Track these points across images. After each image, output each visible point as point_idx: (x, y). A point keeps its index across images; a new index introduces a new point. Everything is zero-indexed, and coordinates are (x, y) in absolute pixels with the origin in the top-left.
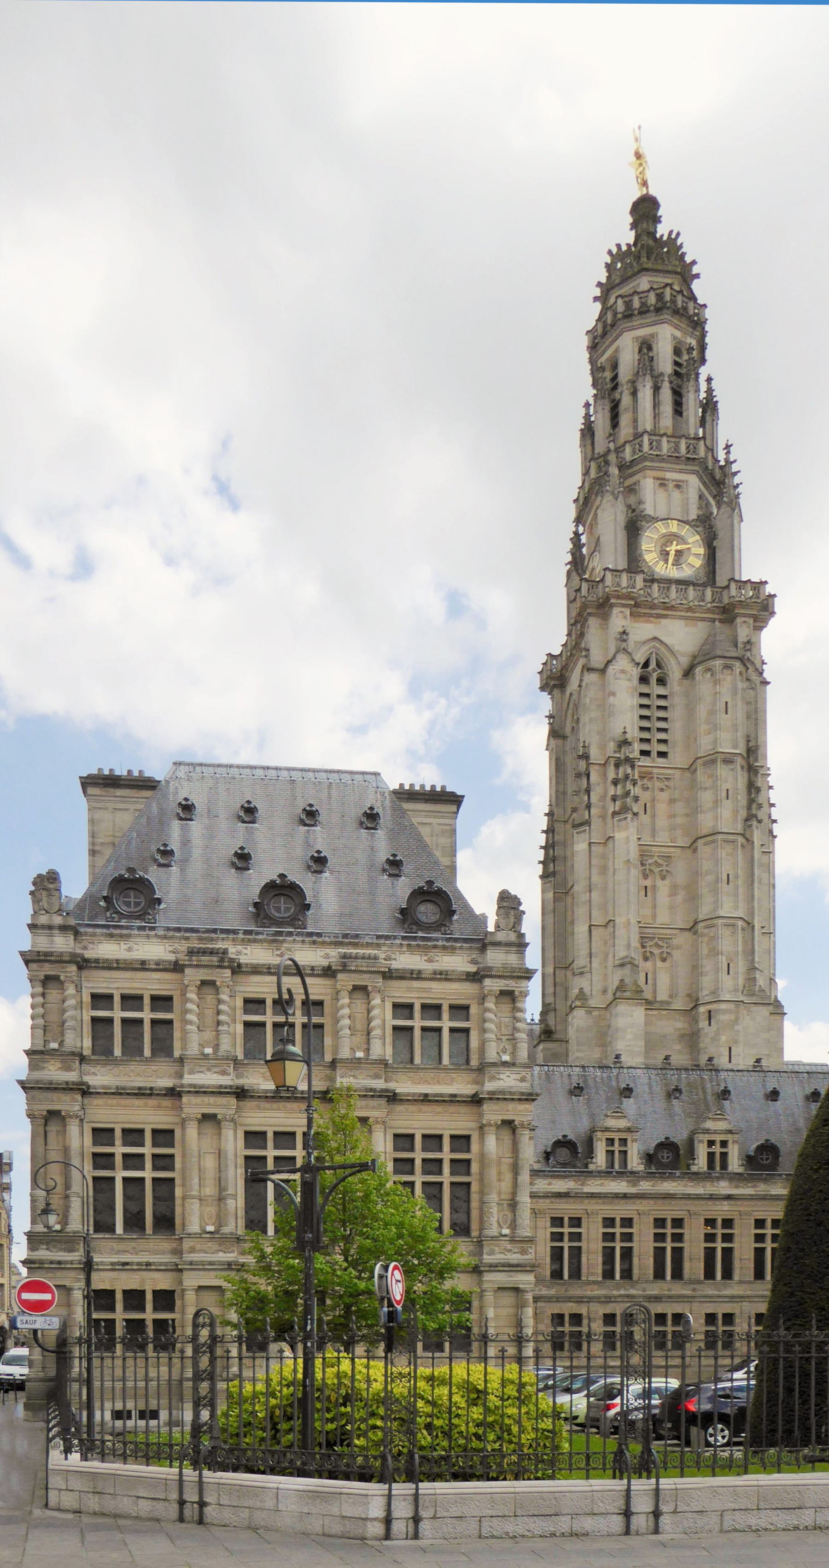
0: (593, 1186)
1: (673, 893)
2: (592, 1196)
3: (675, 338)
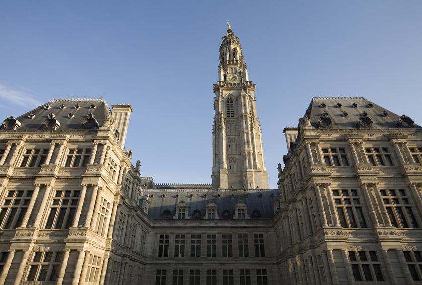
0: (204, 225)
2: (202, 227)
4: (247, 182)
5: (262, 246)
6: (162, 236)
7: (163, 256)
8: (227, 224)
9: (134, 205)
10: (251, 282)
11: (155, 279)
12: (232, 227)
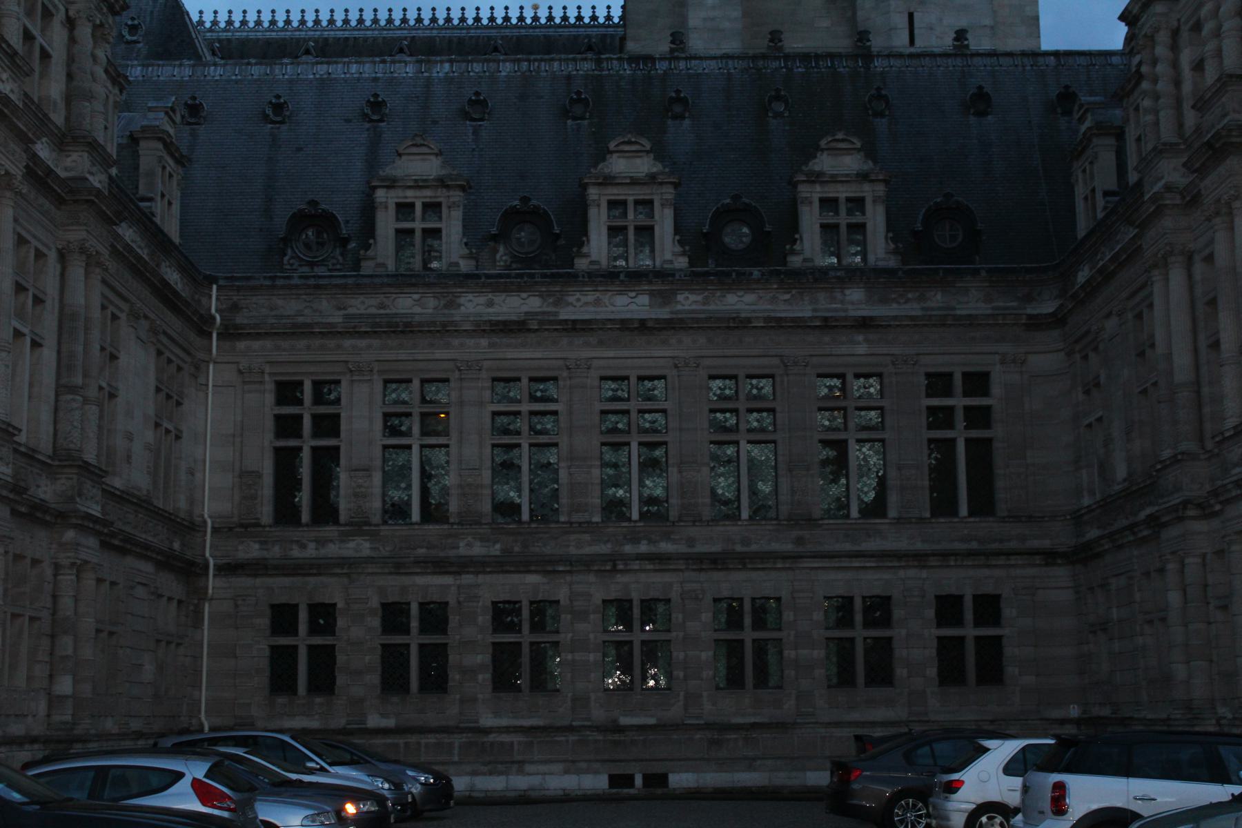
0: (581, 305)
2: (576, 327)
5: (981, 453)
6: (287, 391)
7: (305, 517)
8: (739, 302)
9: (97, 180)
10: (900, 672)
11: (264, 663)
12: (777, 324)
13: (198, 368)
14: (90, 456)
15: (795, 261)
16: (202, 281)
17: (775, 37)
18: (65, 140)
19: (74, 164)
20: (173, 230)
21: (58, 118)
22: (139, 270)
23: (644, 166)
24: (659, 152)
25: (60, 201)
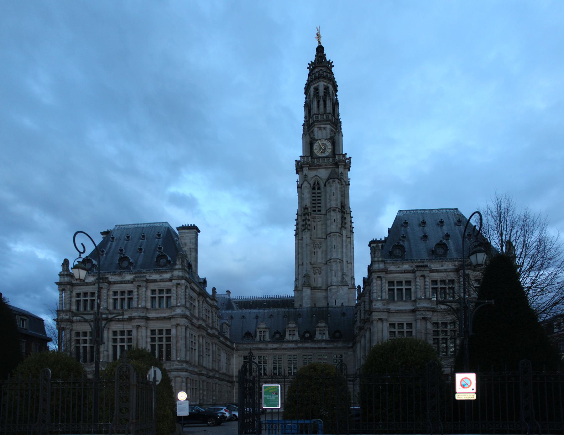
0: (285, 346)
1: (322, 253)
2: (284, 349)
3: (324, 85)
4: (331, 298)
8: (307, 345)
9: (216, 333)
12: (312, 348)
13: (233, 355)
14: (217, 369)
15: (315, 339)
16: (232, 343)
17: (315, 304)
18: (212, 328)
19: (214, 331)
20: (228, 337)
21: (211, 326)
22: (223, 343)
23: (294, 325)
24: (296, 323)
25: (211, 337)
